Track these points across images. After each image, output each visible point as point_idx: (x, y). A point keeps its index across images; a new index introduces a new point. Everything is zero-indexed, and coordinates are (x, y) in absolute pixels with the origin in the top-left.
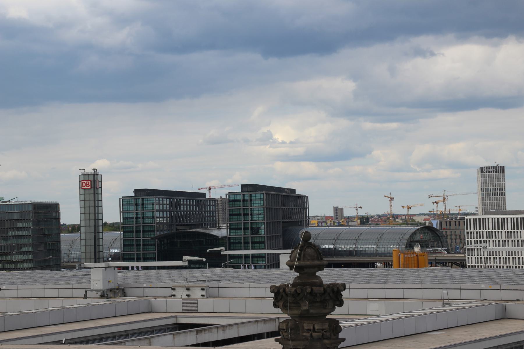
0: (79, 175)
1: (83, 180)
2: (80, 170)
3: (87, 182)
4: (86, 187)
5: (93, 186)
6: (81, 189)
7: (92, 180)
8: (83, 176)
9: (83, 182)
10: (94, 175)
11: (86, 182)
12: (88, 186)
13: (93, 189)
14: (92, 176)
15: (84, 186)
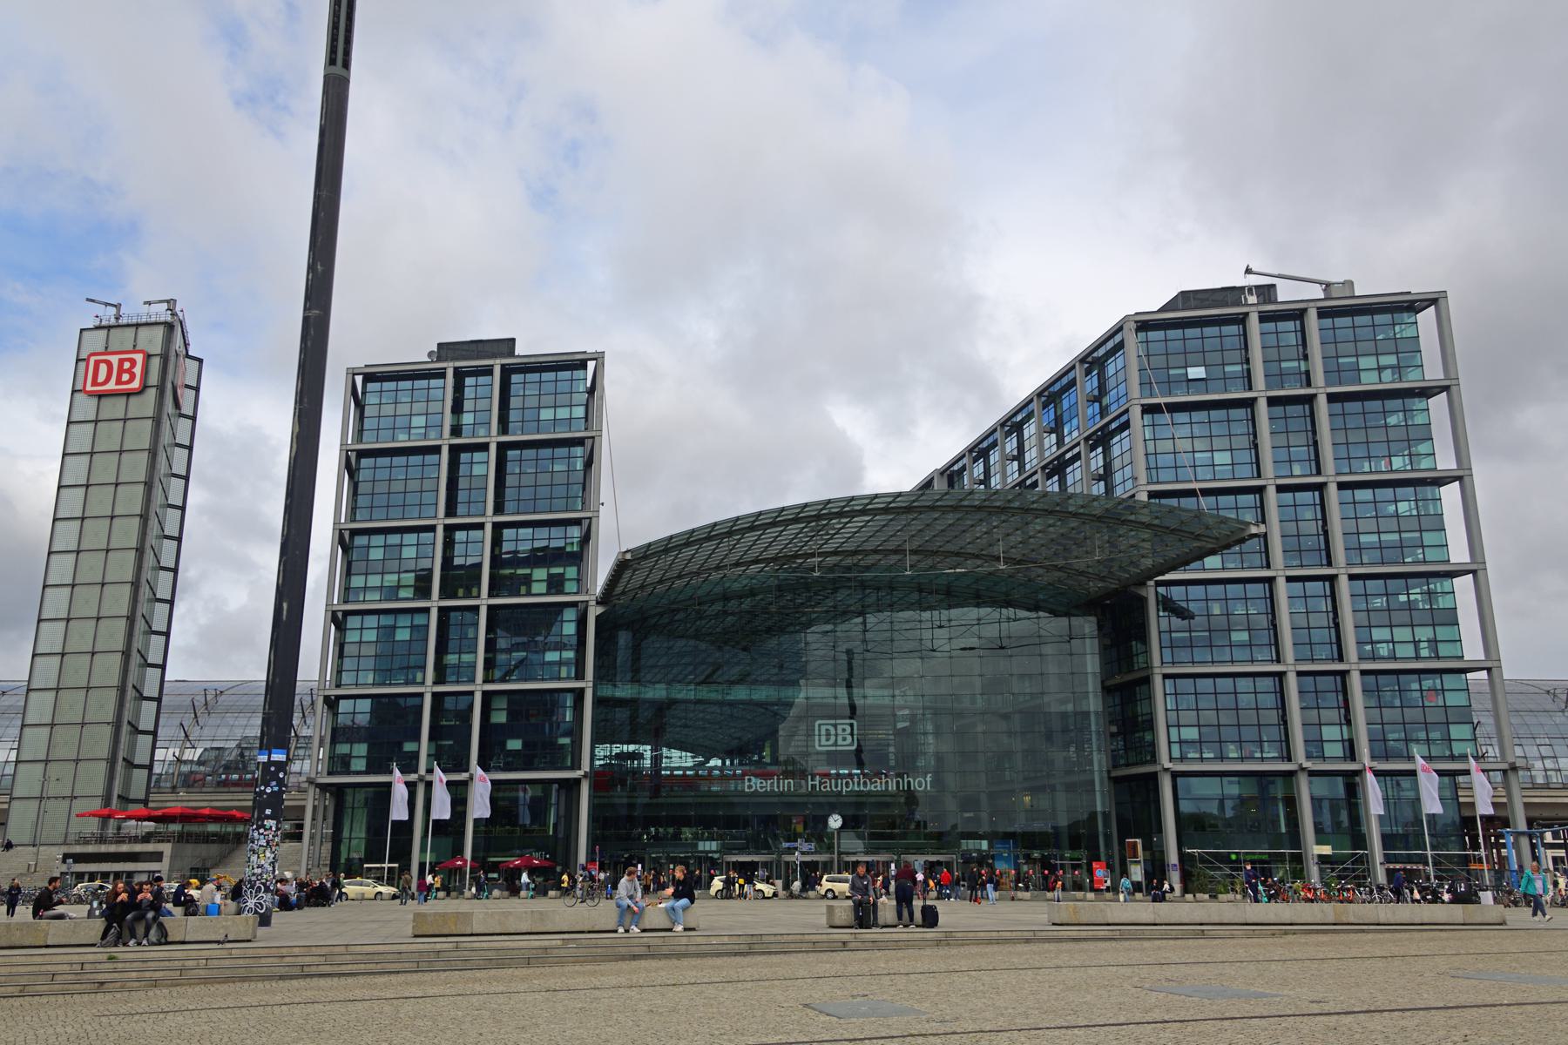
0: (82, 330)
1: (103, 350)
2: (93, 301)
3: (121, 362)
4: (112, 386)
5: (154, 379)
6: (77, 395)
7: (157, 349)
8: (103, 333)
9: (97, 363)
10: (169, 327)
11: (114, 359)
12: (126, 377)
13: (152, 393)
14: (159, 332)
15: (101, 378)
